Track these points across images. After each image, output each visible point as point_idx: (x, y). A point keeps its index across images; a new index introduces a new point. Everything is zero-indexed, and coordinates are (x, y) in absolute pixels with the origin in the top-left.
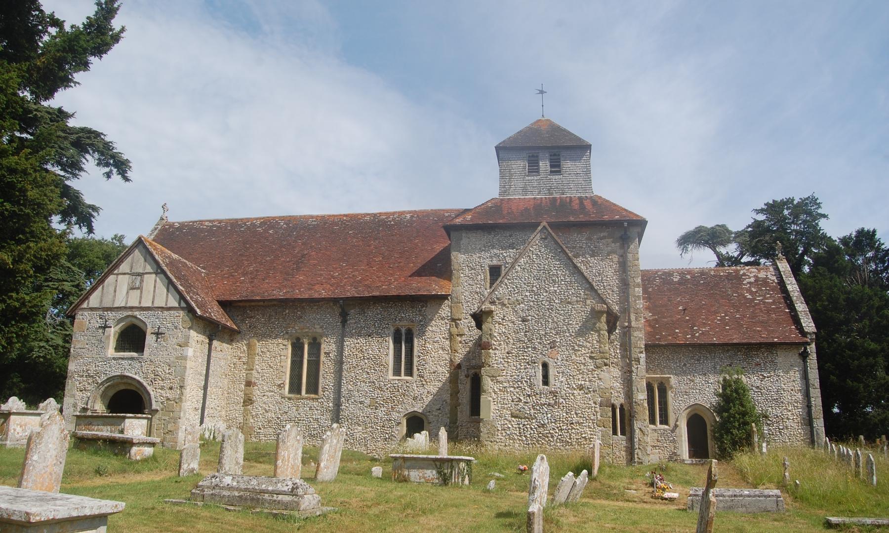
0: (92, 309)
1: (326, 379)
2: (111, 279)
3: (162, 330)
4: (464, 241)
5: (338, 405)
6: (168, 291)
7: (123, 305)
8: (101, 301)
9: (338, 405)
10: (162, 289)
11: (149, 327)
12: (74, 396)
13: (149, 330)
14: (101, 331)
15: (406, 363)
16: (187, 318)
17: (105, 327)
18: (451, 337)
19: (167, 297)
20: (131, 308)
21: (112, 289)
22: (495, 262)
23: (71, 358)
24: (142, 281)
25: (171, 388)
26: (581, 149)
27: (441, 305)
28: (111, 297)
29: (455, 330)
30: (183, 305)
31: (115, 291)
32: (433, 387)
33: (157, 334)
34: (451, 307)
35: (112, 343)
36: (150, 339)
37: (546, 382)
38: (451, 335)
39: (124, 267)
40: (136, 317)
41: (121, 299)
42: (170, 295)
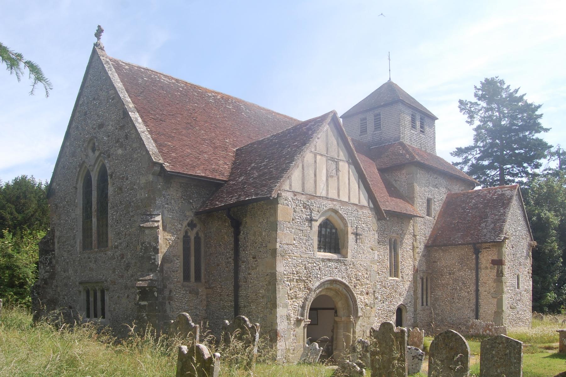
0: (295, 193)
6: (359, 187)
7: (324, 194)
8: (303, 184)
10: (355, 185)
11: (349, 225)
13: (350, 230)
16: (374, 220)
17: (311, 220)
18: (414, 248)
19: (359, 191)
20: (332, 200)
21: (312, 173)
23: (279, 258)
24: (337, 170)
27: (409, 222)
28: (312, 181)
29: (414, 243)
30: (372, 205)
31: (315, 175)
32: (407, 285)
33: (356, 234)
34: (413, 226)
38: (413, 247)
40: (336, 212)
41: (322, 187)
42: (361, 193)
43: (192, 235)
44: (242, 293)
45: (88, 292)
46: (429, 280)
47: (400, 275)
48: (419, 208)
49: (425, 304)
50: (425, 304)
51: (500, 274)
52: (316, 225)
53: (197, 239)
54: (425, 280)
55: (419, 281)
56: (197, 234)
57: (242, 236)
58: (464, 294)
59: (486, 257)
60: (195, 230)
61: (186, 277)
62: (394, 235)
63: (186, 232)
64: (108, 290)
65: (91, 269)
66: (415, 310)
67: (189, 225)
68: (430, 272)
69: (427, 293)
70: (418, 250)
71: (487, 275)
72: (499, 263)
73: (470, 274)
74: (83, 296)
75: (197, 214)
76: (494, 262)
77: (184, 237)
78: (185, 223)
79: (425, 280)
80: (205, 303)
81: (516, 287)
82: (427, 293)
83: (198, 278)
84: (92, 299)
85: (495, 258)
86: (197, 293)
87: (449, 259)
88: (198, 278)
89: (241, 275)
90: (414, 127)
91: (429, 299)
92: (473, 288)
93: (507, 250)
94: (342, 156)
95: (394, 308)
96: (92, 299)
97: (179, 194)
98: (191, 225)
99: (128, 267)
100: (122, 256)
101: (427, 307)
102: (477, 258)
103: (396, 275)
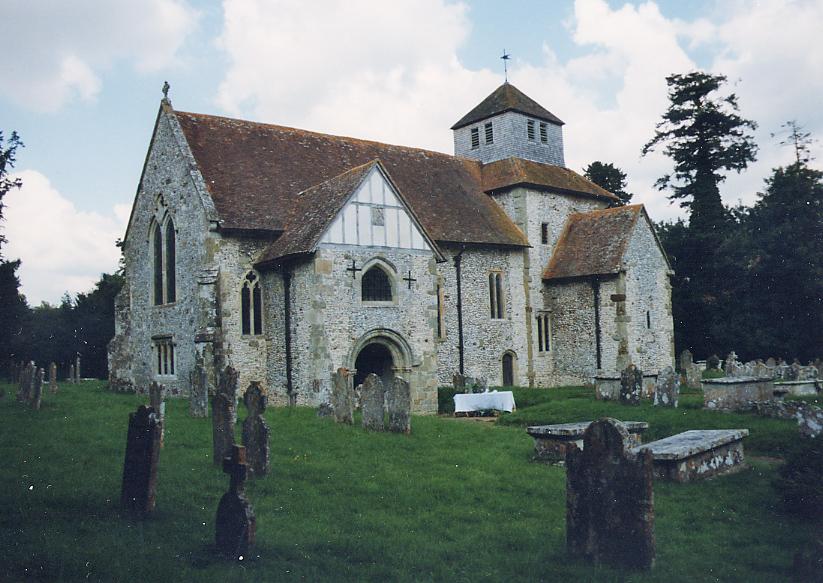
1: (450, 324)
2: (349, 210)
3: (413, 276)
4: (528, 198)
5: (461, 348)
9: (461, 348)
11: (399, 271)
12: (328, 356)
14: (349, 273)
15: (497, 308)
17: (354, 269)
22: (546, 221)
25: (426, 341)
26: (560, 124)
35: (358, 289)
36: (399, 286)
37: (649, 327)
39: (363, 195)
43: (251, 286)
44: (293, 344)
45: (159, 348)
46: (549, 320)
47: (505, 314)
48: (533, 237)
49: (544, 348)
50: (544, 348)
51: (621, 311)
52: (359, 275)
53: (257, 291)
54: (543, 321)
55: (535, 322)
56: (257, 284)
57: (291, 288)
58: (586, 336)
59: (607, 291)
60: (254, 283)
61: (246, 330)
62: (497, 269)
63: (245, 284)
64: (175, 345)
65: (162, 325)
66: (530, 356)
67: (247, 277)
68: (549, 310)
69: (547, 336)
70: (530, 285)
71: (608, 313)
72: (619, 298)
73: (589, 311)
74: (156, 349)
75: (256, 266)
76: (614, 298)
77: (243, 290)
78: (244, 276)
79: (543, 321)
80: (265, 355)
81: (646, 326)
82: (547, 336)
83: (258, 330)
84: (162, 355)
85: (614, 293)
86: (257, 345)
87: (569, 296)
88: (258, 330)
89: (292, 327)
90: (531, 137)
91: (550, 343)
92: (594, 329)
93: (630, 285)
94: (391, 199)
95: (499, 355)
96: (162, 355)
97: (237, 248)
98: (250, 277)
99: (192, 321)
100: (187, 311)
101: (547, 353)
102: (597, 293)
103: (500, 317)
